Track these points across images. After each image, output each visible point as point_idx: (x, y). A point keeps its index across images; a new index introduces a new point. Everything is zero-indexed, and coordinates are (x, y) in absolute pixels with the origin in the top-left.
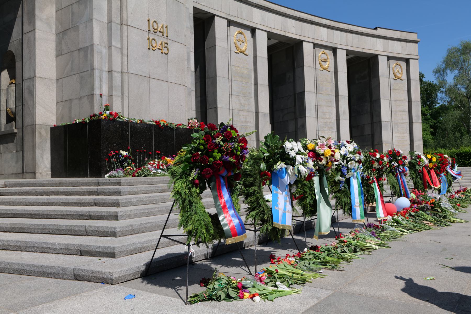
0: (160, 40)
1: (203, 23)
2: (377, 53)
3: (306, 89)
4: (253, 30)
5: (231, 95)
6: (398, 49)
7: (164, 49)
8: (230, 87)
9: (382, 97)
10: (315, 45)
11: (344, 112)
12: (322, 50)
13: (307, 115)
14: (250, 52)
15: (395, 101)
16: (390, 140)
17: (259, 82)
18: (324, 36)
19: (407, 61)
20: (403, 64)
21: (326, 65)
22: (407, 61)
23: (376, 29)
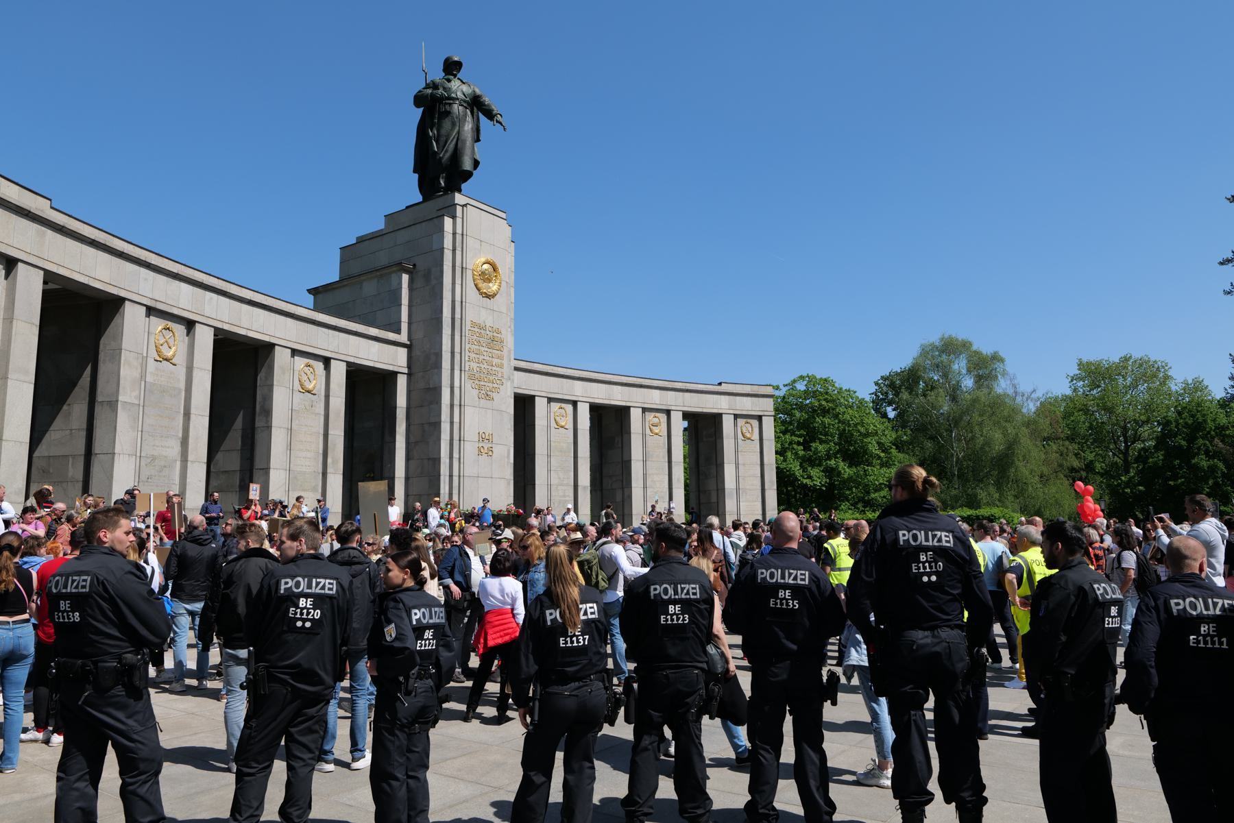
1: (524, 406)
3: (633, 457)
4: (575, 403)
5: (549, 471)
6: (746, 406)
8: (549, 462)
10: (644, 410)
12: (653, 414)
13: (634, 484)
14: (570, 426)
17: (580, 454)
18: (655, 398)
19: (760, 418)
20: (755, 423)
21: (656, 430)
22: (760, 418)
23: (720, 384)
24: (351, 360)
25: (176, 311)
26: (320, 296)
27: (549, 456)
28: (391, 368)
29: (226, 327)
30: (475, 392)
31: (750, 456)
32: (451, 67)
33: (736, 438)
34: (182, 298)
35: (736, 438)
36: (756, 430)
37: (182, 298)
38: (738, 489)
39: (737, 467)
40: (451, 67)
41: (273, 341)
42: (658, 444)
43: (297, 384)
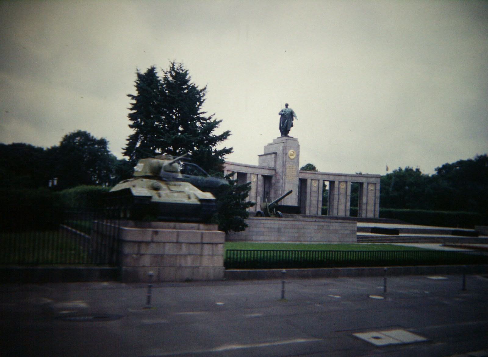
4: (319, 180)
9: (364, 195)
18: (343, 178)
26: (260, 157)
27: (311, 193)
31: (371, 195)
32: (287, 106)
38: (367, 203)
39: (367, 197)
40: (287, 106)
42: (342, 191)
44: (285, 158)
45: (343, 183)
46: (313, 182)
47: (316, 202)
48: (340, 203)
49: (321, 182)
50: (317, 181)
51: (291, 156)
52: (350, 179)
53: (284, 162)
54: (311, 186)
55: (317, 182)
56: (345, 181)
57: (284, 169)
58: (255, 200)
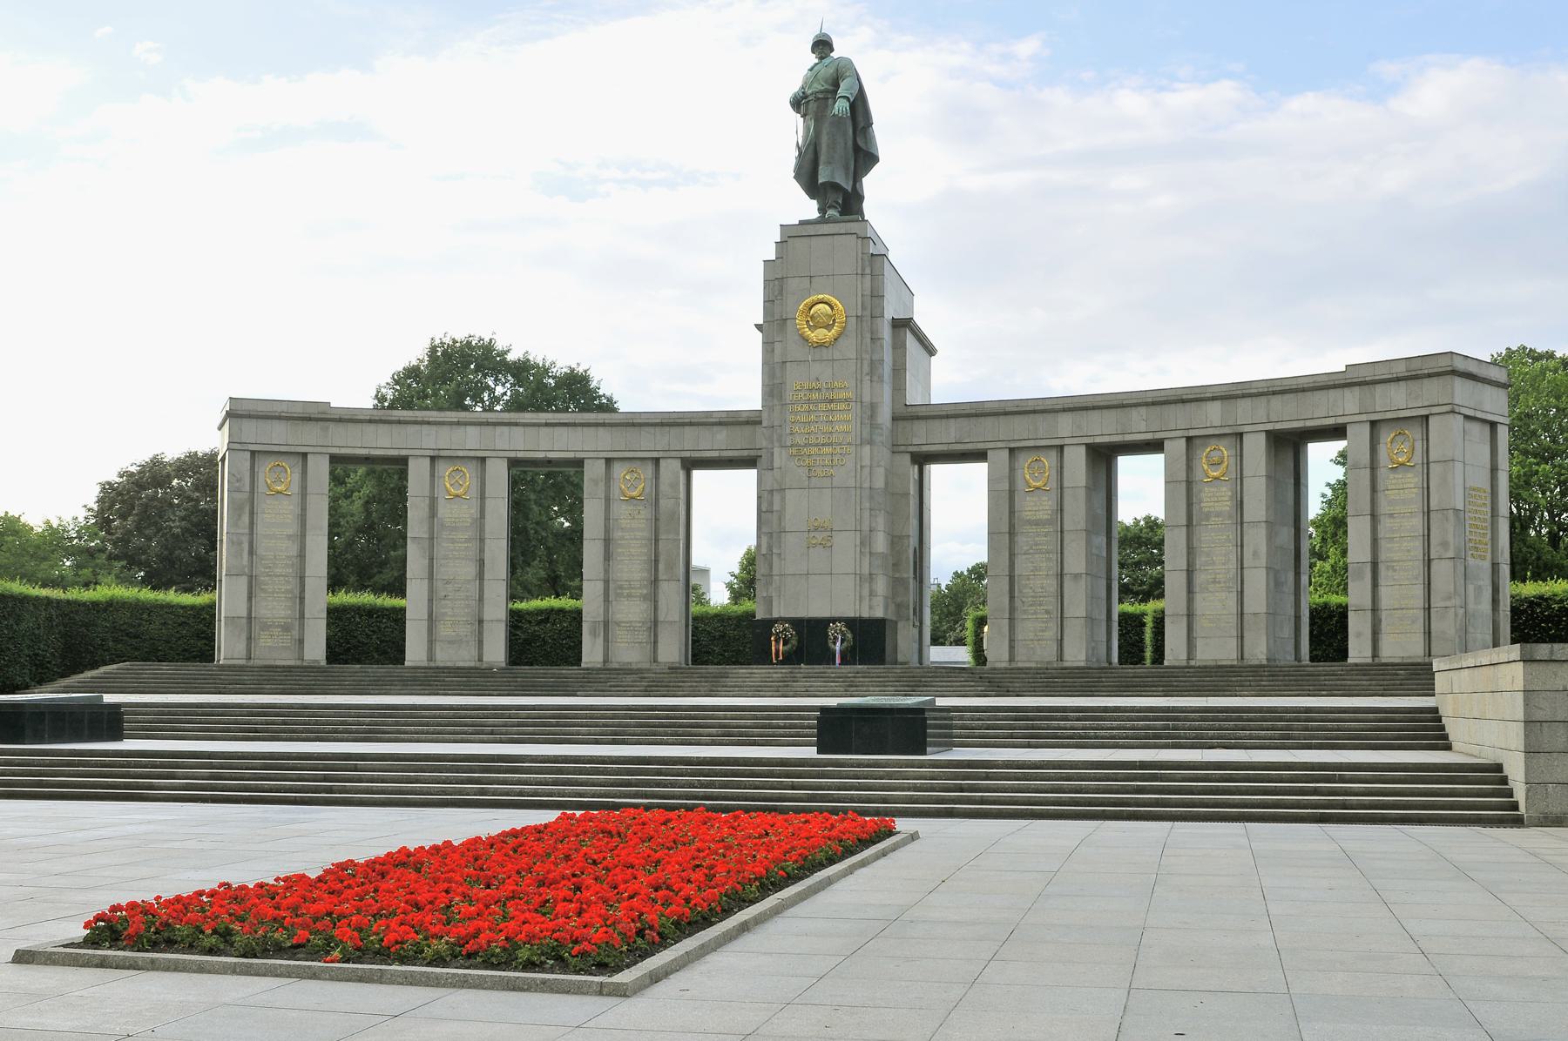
0: (819, 536)
2: (1340, 420)
4: (1061, 447)
6: (1396, 399)
7: (827, 545)
11: (1255, 554)
15: (1391, 515)
16: (1368, 604)
18: (1213, 415)
24: (687, 454)
25: (461, 454)
28: (745, 453)
29: (520, 455)
30: (803, 473)
33: (1373, 467)
34: (470, 440)
35: (1373, 467)
36: (1418, 445)
37: (470, 440)
38: (1375, 565)
39: (1374, 516)
41: (580, 455)
43: (617, 492)
44: (778, 351)
45: (1213, 444)
46: (1025, 461)
47: (1052, 585)
48: (1200, 578)
49: (1077, 460)
50: (1053, 454)
51: (816, 327)
52: (1261, 414)
53: (778, 373)
54: (1012, 493)
55: (1048, 461)
56: (1227, 430)
57: (777, 408)
58: (644, 598)
